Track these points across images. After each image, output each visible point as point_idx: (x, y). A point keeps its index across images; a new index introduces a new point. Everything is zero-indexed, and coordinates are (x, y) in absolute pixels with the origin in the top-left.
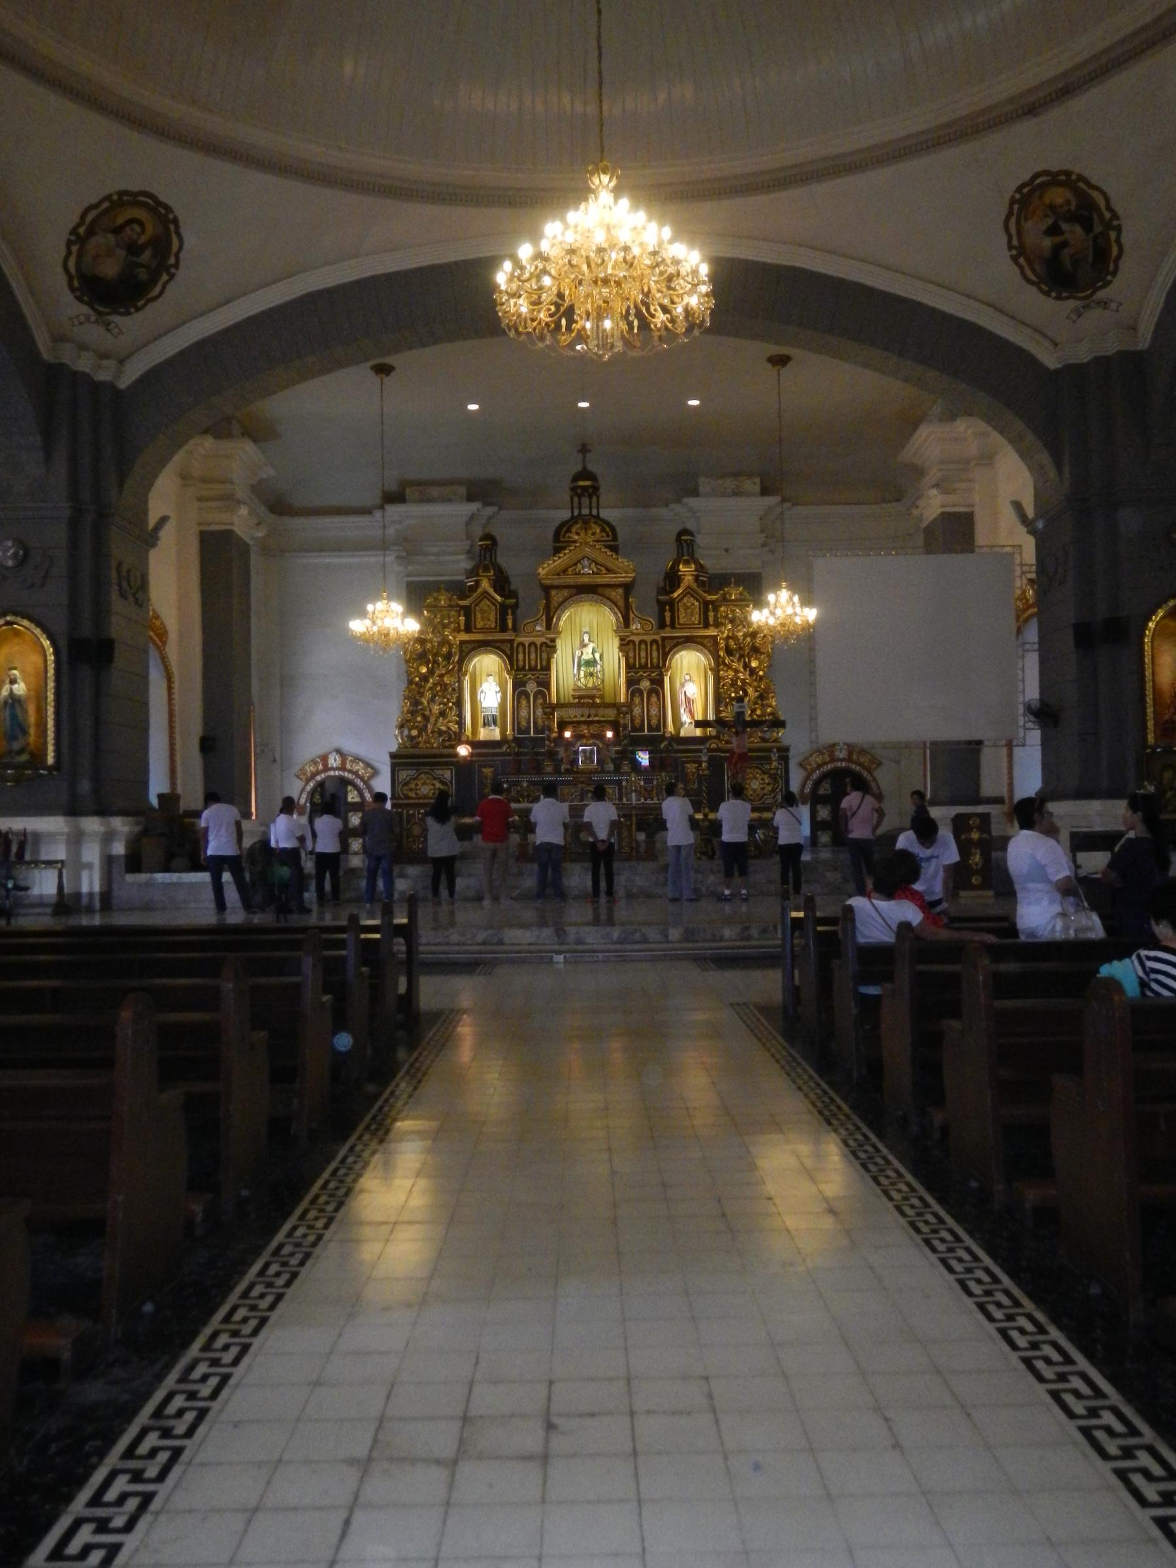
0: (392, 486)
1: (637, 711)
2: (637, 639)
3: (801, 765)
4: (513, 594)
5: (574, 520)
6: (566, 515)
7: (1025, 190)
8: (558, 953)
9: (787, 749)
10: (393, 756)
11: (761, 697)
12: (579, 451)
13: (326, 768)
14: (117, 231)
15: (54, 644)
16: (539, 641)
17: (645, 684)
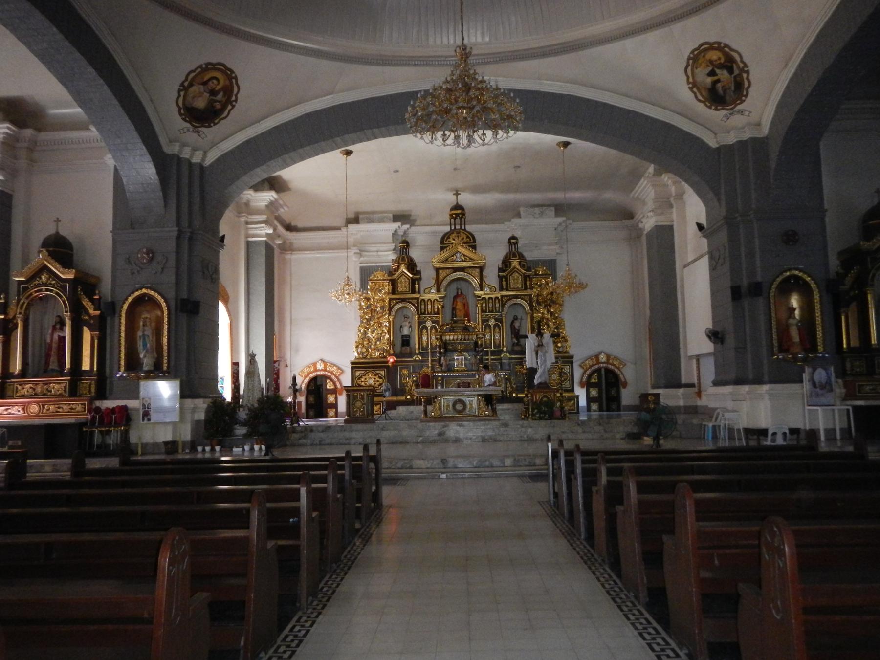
0: (353, 216)
1: (488, 336)
2: (487, 297)
3: (580, 366)
4: (419, 273)
5: (451, 232)
6: (447, 229)
7: (696, 53)
8: (443, 473)
9: (572, 357)
10: (352, 363)
11: (557, 328)
13: (316, 370)
14: (205, 83)
15: (168, 305)
16: (433, 298)
17: (492, 322)
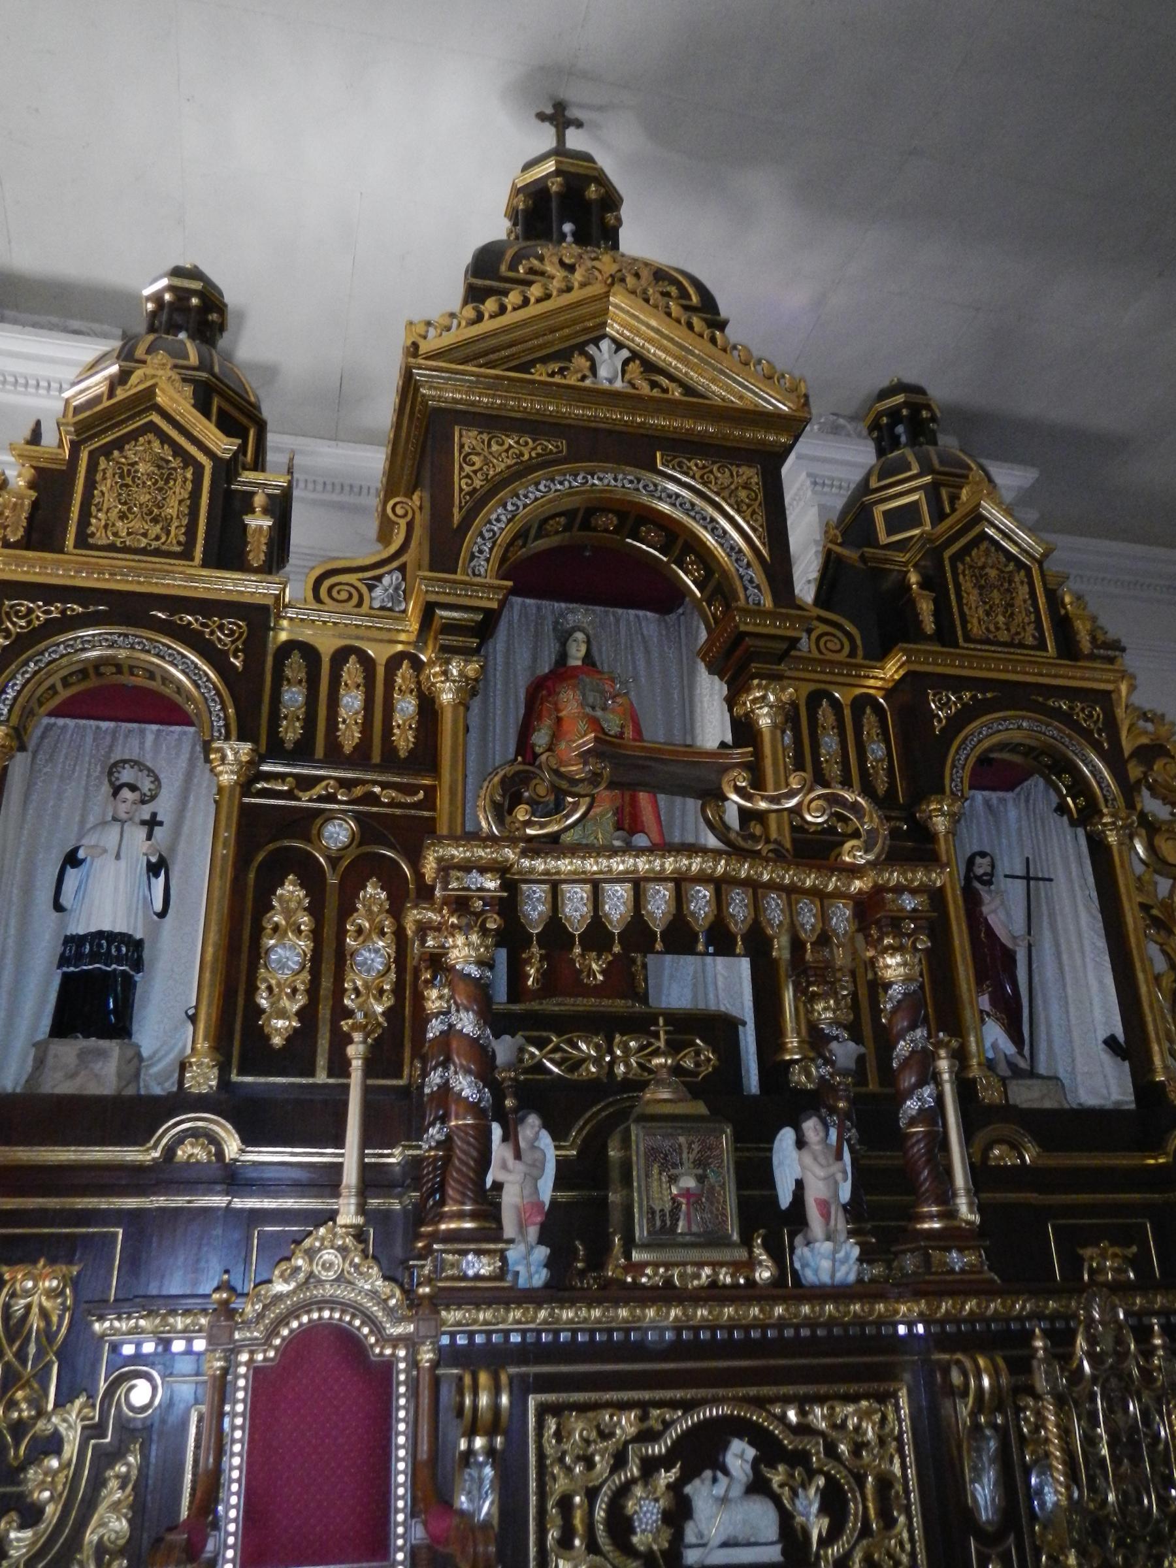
12: (542, 117)
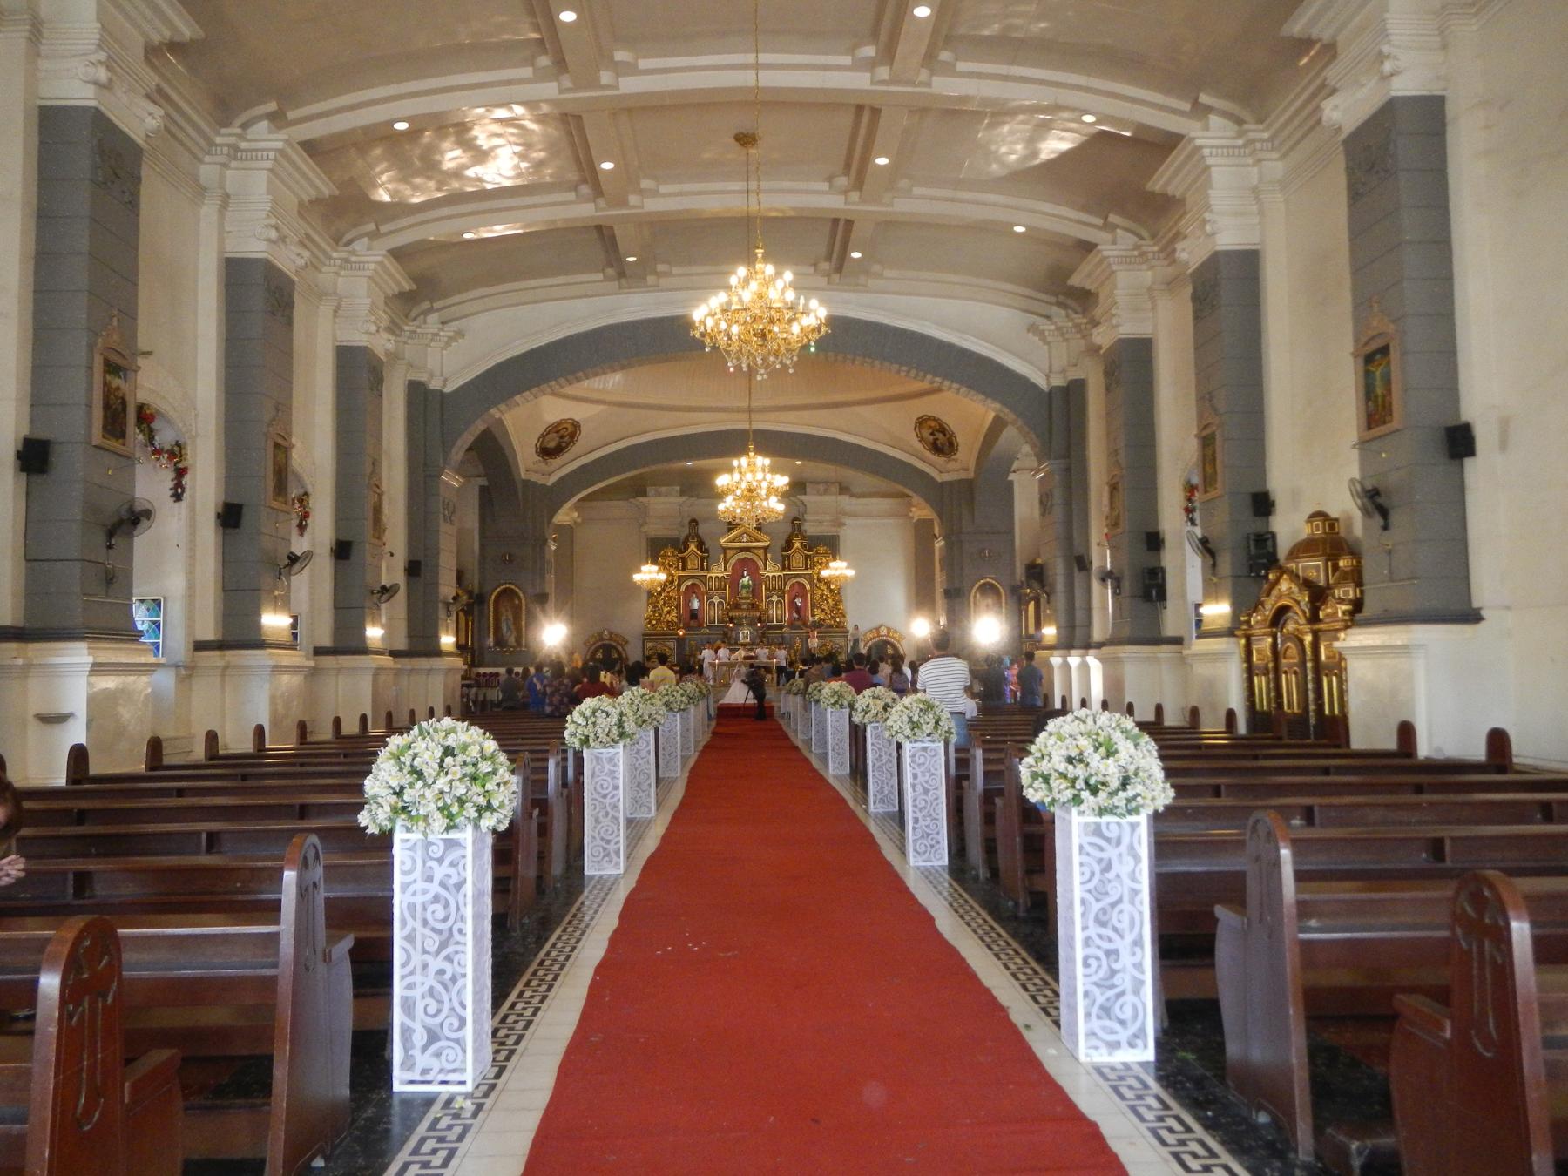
4: (707, 551)
13: (602, 639)
17: (775, 599)
